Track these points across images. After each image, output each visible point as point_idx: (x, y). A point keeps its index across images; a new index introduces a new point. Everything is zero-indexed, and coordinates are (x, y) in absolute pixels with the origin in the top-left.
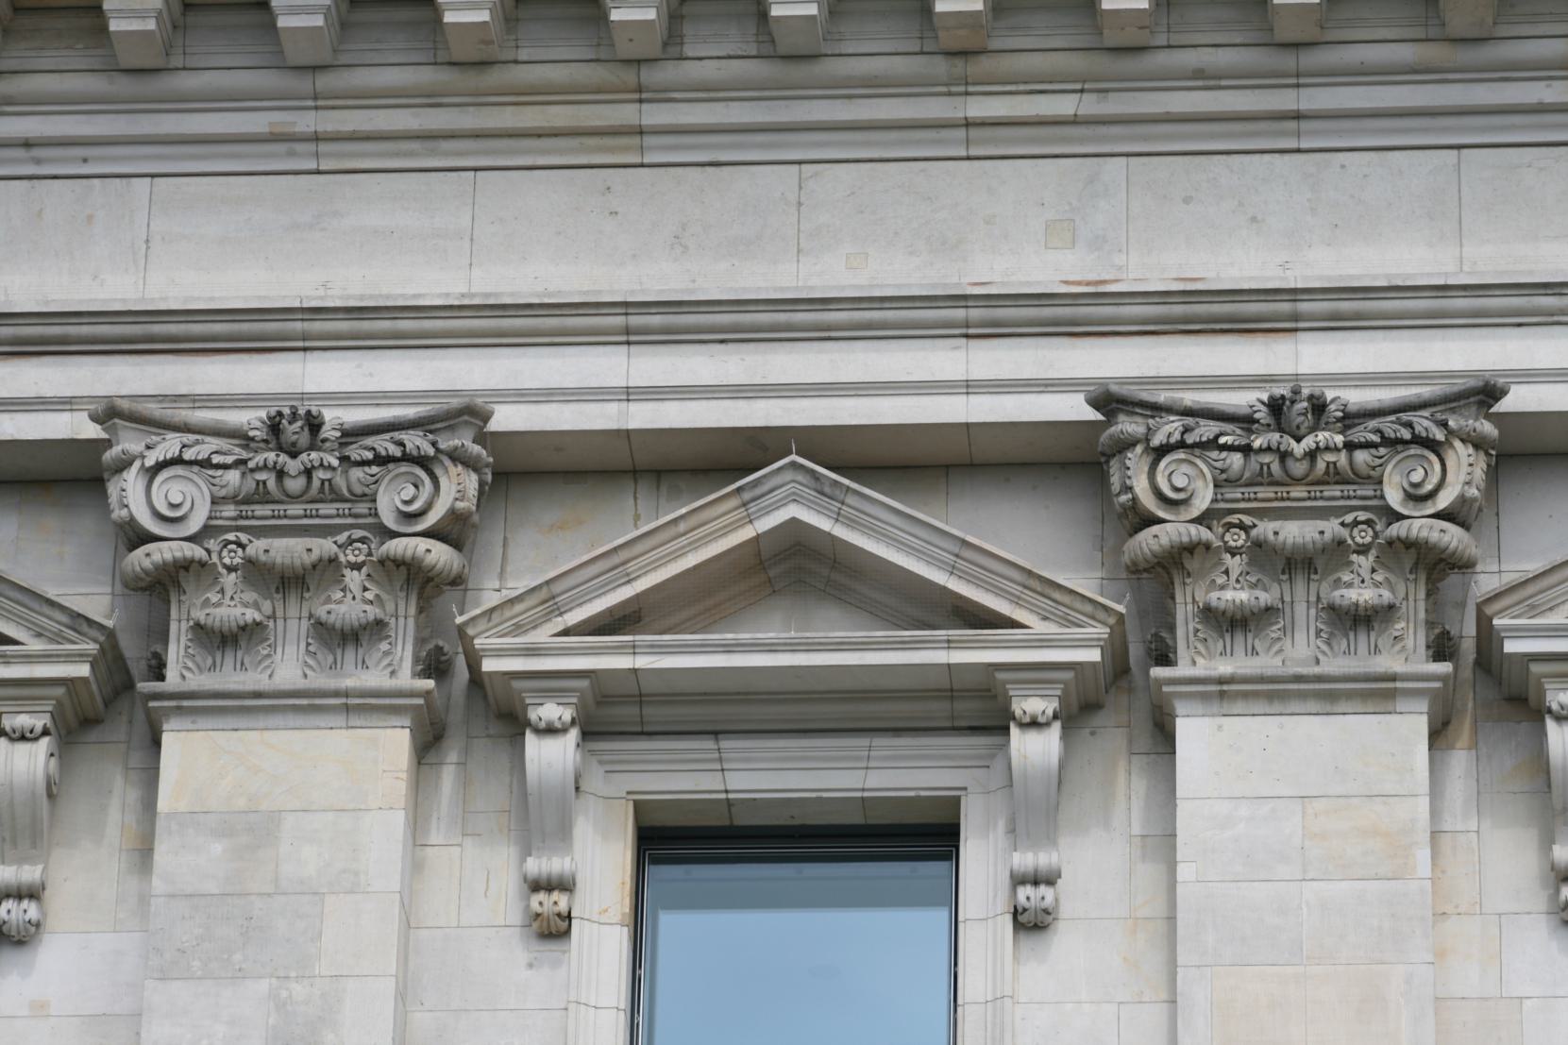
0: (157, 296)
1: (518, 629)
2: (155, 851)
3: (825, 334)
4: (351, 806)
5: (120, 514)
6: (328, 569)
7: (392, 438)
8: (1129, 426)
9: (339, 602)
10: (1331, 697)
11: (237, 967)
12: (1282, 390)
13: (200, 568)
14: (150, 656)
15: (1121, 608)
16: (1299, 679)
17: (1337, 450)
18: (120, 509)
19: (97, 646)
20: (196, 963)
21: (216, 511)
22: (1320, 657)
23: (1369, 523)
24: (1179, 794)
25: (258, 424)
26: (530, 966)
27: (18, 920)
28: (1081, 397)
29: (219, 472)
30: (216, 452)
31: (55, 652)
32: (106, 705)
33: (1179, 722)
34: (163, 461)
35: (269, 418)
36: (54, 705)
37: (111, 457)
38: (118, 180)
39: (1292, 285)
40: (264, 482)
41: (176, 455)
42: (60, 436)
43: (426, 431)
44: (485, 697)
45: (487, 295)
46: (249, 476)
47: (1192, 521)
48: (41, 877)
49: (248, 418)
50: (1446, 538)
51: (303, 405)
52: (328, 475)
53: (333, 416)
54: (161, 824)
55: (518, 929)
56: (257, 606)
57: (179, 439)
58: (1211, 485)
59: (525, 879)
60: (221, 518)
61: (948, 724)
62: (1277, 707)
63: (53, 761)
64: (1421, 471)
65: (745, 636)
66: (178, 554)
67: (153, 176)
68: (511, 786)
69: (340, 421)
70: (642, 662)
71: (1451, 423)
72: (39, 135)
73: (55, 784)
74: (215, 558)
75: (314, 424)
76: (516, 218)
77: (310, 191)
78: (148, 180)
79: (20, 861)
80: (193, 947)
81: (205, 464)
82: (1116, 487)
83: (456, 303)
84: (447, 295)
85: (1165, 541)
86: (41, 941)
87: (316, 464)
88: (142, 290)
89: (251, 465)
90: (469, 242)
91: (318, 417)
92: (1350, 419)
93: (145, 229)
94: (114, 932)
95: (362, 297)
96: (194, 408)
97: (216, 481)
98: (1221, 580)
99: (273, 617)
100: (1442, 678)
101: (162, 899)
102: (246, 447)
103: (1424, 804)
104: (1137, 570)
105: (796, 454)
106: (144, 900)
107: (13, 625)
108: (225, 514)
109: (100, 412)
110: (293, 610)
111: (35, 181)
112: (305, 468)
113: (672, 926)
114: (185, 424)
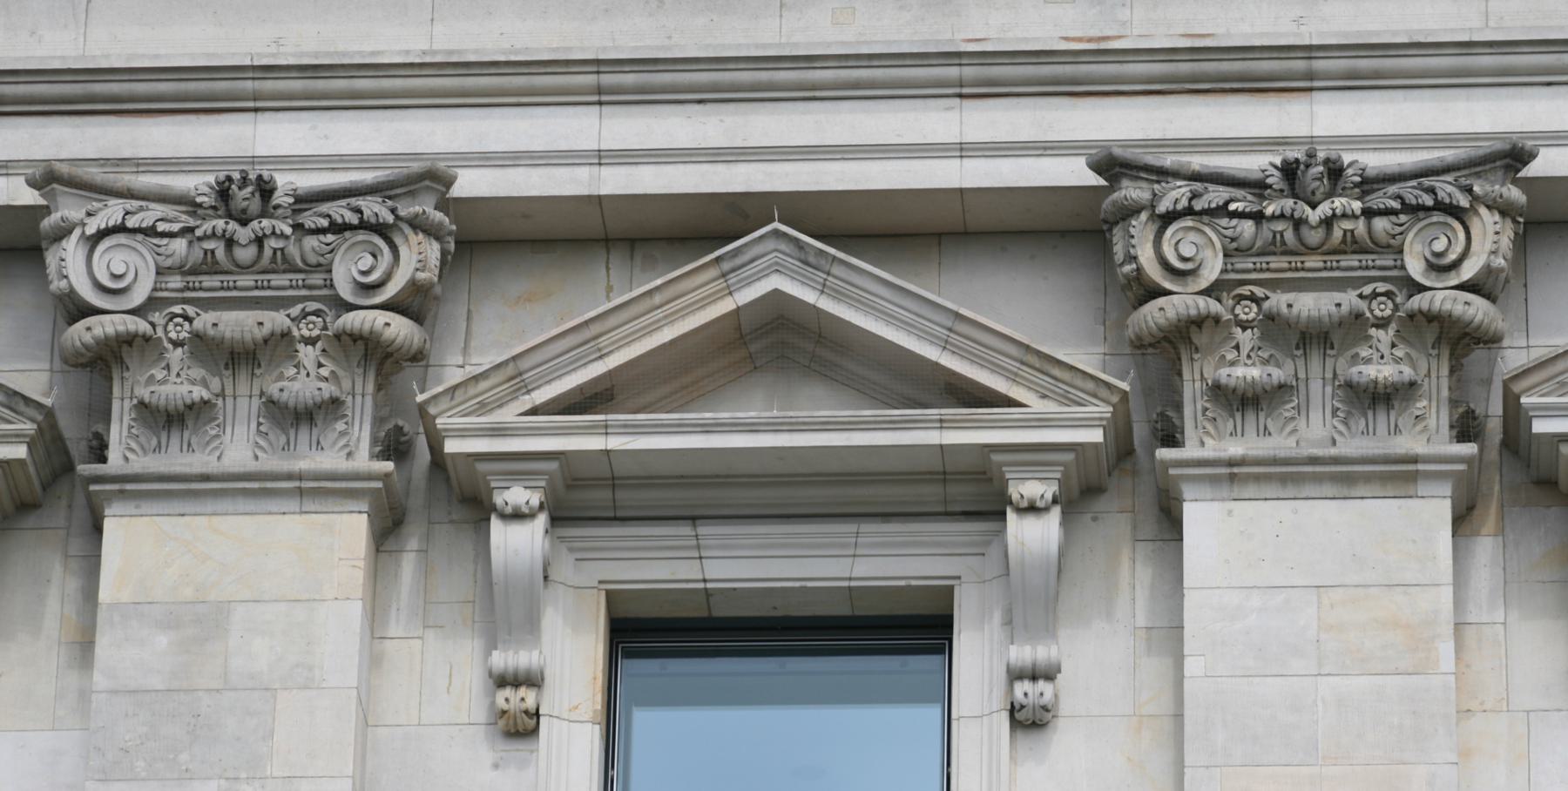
0: (98, 53)
1: (483, 408)
3: (810, 94)
5: (58, 285)
6: (281, 344)
7: (348, 204)
8: (1133, 191)
9: (292, 379)
10: (1348, 480)
11: (184, 768)
13: (144, 343)
14: (91, 435)
15: (1125, 386)
16: (1314, 461)
17: (1354, 217)
18: (59, 280)
19: (35, 426)
21: (161, 282)
22: (1337, 437)
23: (1388, 294)
24: (1186, 583)
25: (206, 190)
26: (496, 766)
28: (1082, 161)
29: (165, 241)
30: (161, 220)
32: (45, 487)
34: (104, 229)
35: (218, 183)
37: (50, 225)
39: (1307, 42)
40: (213, 252)
41: (118, 223)
43: (385, 197)
44: (448, 479)
45: (451, 52)
46: (196, 245)
47: (1200, 293)
49: (194, 184)
50: (1471, 311)
51: (254, 169)
52: (279, 244)
53: (286, 181)
56: (205, 384)
57: (121, 206)
58: (1221, 255)
59: (490, 674)
60: (167, 290)
61: (940, 509)
62: (1290, 491)
64: (1444, 240)
65: (724, 415)
66: (121, 328)
68: (475, 575)
70: (615, 443)
71: (1476, 189)
74: (160, 332)
75: (265, 190)
80: (137, 745)
81: (150, 232)
83: (417, 60)
84: (407, 52)
85: (1171, 314)
87: (268, 232)
88: (82, 46)
89: (199, 233)
91: (270, 181)
92: (1369, 184)
95: (316, 54)
96: (138, 172)
97: (161, 250)
98: (1231, 356)
99: (222, 394)
101: (104, 695)
102: (193, 214)
103: (1447, 594)
104: (1140, 345)
106: (84, 696)
108: (171, 285)
109: (37, 177)
112: (257, 236)
114: (129, 190)
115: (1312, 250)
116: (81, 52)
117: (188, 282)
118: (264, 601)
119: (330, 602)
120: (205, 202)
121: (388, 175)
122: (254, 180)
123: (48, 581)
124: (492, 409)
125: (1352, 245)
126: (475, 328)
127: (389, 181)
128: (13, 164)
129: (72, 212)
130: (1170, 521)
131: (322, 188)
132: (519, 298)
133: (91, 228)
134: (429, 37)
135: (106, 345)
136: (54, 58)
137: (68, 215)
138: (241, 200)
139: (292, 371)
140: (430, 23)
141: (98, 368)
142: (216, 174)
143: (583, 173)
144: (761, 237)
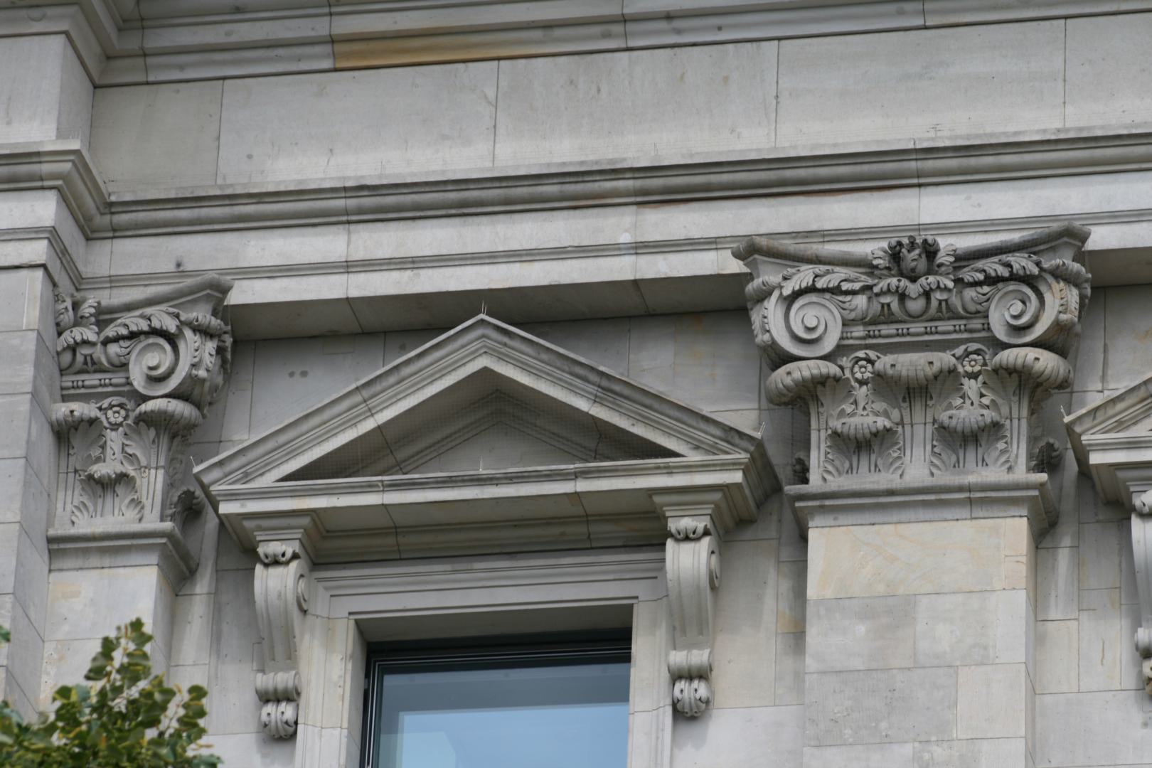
0: (787, 145)
1: (1120, 425)
2: (807, 633)
4: (978, 588)
5: (762, 338)
6: (948, 379)
7: (1000, 260)
9: (960, 408)
11: (884, 734)
13: (835, 383)
18: (763, 334)
19: (748, 456)
20: (848, 732)
21: (847, 332)
25: (881, 254)
26: (1145, 725)
27: (690, 698)
29: (849, 298)
31: (711, 462)
32: (759, 505)
34: (798, 291)
35: (890, 248)
36: (713, 509)
37: (754, 289)
38: (749, 45)
40: (889, 305)
41: (809, 285)
42: (708, 273)
43: (1031, 253)
44: (1093, 486)
45: (1081, 129)
46: (875, 300)
48: (709, 660)
49: (872, 249)
51: (920, 235)
52: (944, 296)
53: (947, 243)
54: (810, 610)
55: (1133, 692)
56: (886, 414)
57: (811, 271)
59: (1137, 648)
60: (852, 338)
63: (714, 557)
66: (815, 372)
67: (779, 39)
68: (1120, 565)
69: (954, 248)
72: (679, 8)
73: (717, 578)
74: (848, 374)
75: (930, 251)
76: (1104, 59)
77: (919, 44)
78: (776, 42)
79: (690, 646)
80: (845, 716)
81: (836, 291)
83: (1053, 137)
84: (1045, 131)
86: (711, 716)
87: (934, 287)
88: (773, 140)
89: (876, 290)
90: (1063, 83)
93: (775, 87)
94: (775, 706)
95: (968, 137)
96: (824, 242)
97: (846, 306)
99: (901, 423)
101: (815, 676)
102: (871, 274)
106: (799, 676)
107: (674, 439)
108: (855, 334)
109: (742, 250)
111: (676, 49)
112: (924, 290)
114: (817, 257)
116: (774, 144)
117: (869, 331)
118: (943, 593)
119: (999, 592)
120: (880, 264)
121: (1032, 235)
122: (920, 244)
123: (765, 583)
124: (1129, 425)
126: (1111, 358)
127: (1033, 240)
128: (722, 240)
129: (771, 278)
131: (978, 248)
132: (1147, 332)
133: (787, 289)
134: (1062, 117)
135: (804, 386)
136: (751, 150)
137: (767, 280)
138: (910, 261)
139: (959, 401)
140: (1062, 105)
141: (798, 405)
142: (888, 241)
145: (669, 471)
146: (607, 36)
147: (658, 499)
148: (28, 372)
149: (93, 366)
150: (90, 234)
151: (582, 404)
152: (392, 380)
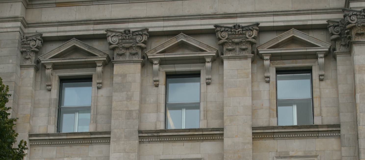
1: (152, 53)
5: (108, 42)
6: (131, 47)
8: (218, 29)
9: (132, 51)
12: (235, 24)
15: (217, 49)
16: (237, 56)
17: (241, 31)
23: (245, 39)
28: (213, 26)
29: (119, 37)
33: (224, 62)
39: (236, 13)
45: (148, 16)
47: (225, 39)
50: (253, 41)
52: (131, 37)
56: (124, 51)
62: (234, 60)
63: (103, 69)
65: (177, 53)
66: (115, 46)
70: (166, 56)
71: (254, 28)
74: (119, 46)
75: (129, 31)
81: (118, 36)
82: (217, 36)
84: (144, 16)
85: (222, 42)
92: (243, 27)
99: (126, 52)
100: (253, 56)
103: (250, 70)
104: (219, 45)
105: (182, 33)
106: (113, 84)
110: (128, 51)
113: (170, 85)
115: (237, 35)
125: (241, 34)
130: (222, 62)
139: (132, 50)
143: (162, 28)
144: (180, 35)
145: (97, 58)
146: (90, 3)
147: (95, 62)
148: (17, 45)
149: (25, 44)
150: (25, 27)
151: (86, 50)
152: (63, 46)
